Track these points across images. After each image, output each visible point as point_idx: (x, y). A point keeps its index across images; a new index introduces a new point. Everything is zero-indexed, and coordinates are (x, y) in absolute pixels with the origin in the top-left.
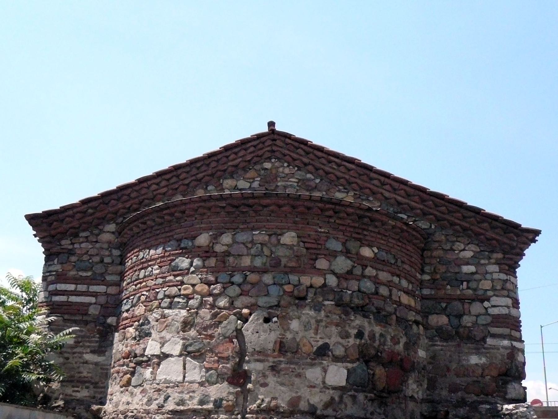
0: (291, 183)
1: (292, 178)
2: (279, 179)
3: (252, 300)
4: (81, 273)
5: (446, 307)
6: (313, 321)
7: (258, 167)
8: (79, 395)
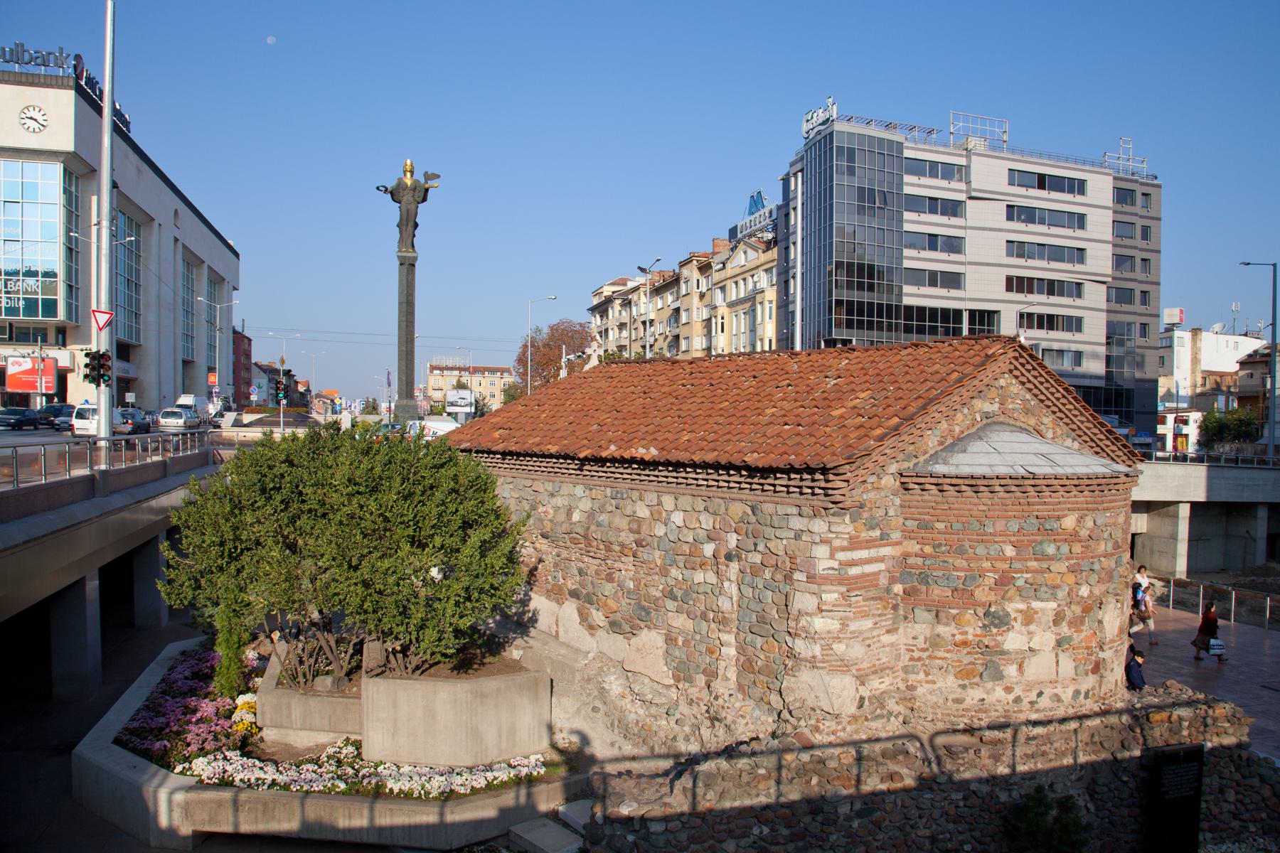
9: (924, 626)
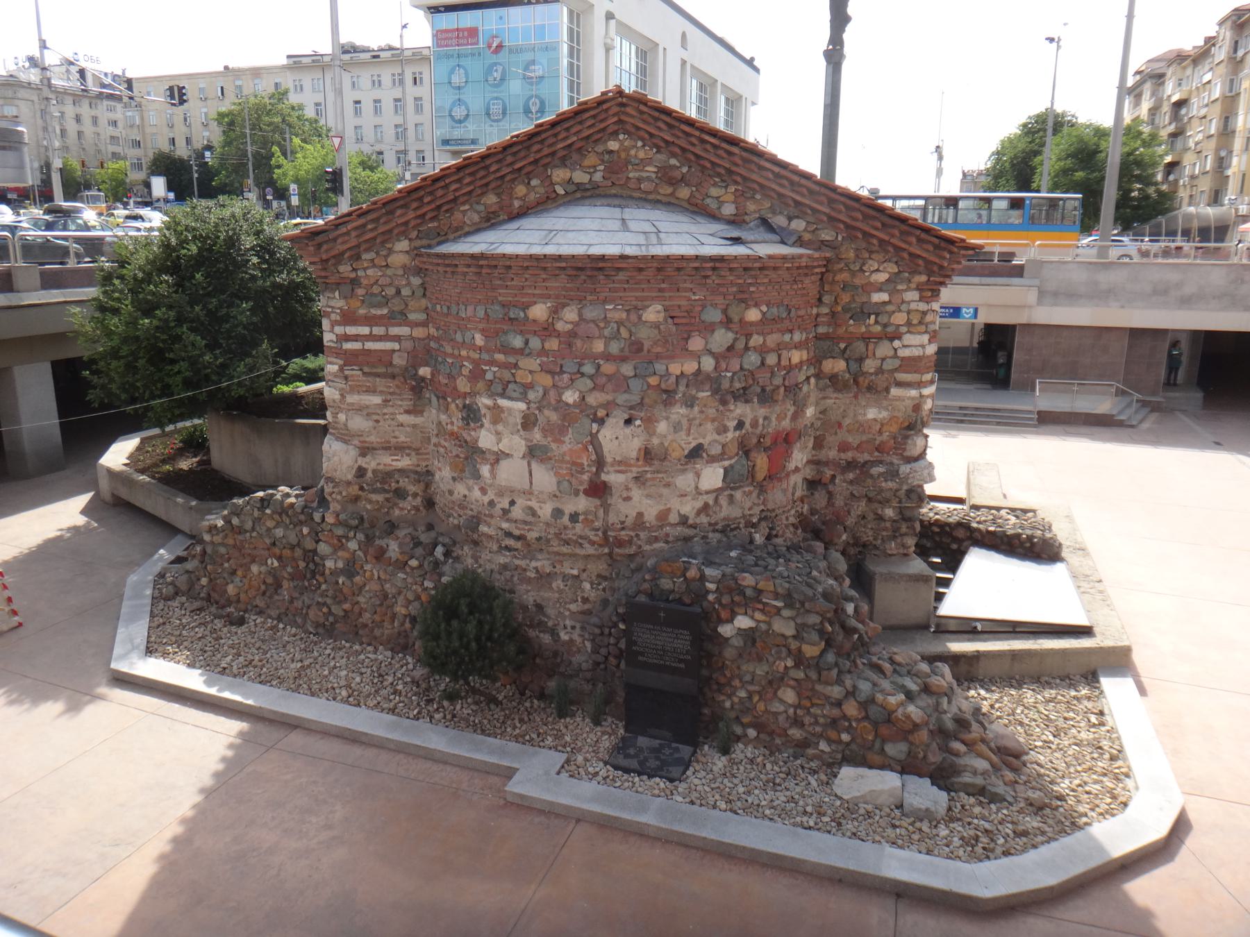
0: (648, 174)
1: (649, 165)
2: (630, 167)
3: (609, 397)
4: (373, 311)
5: (846, 348)
6: (685, 422)
7: (600, 148)
8: (400, 465)
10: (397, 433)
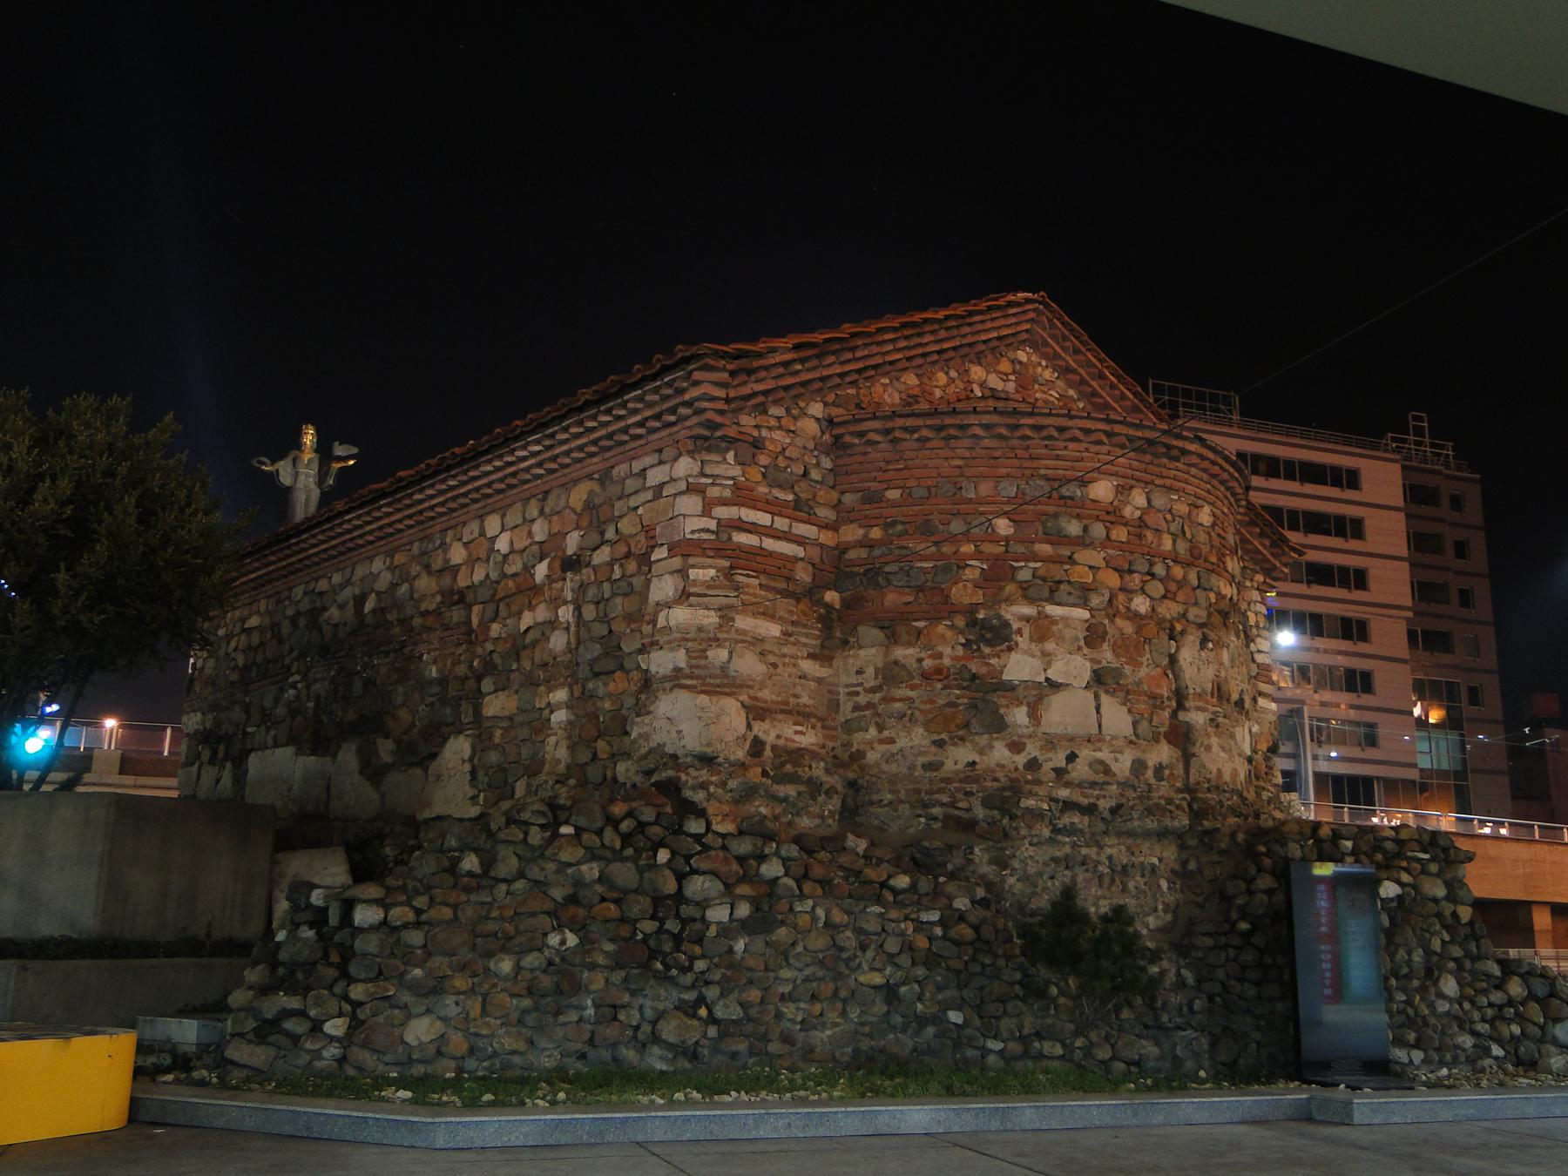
2: (1036, 386)
9: (874, 650)
10: (799, 689)
